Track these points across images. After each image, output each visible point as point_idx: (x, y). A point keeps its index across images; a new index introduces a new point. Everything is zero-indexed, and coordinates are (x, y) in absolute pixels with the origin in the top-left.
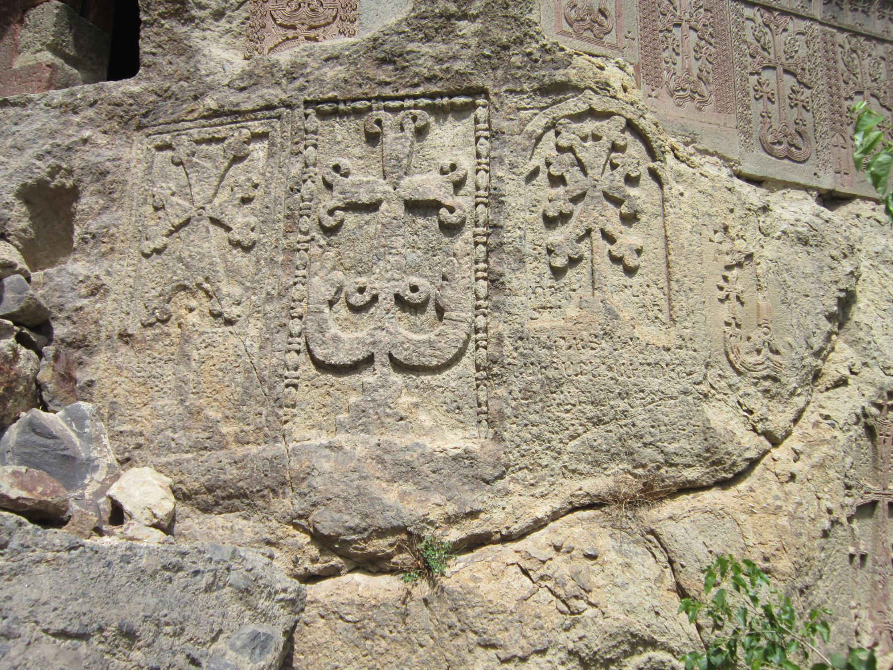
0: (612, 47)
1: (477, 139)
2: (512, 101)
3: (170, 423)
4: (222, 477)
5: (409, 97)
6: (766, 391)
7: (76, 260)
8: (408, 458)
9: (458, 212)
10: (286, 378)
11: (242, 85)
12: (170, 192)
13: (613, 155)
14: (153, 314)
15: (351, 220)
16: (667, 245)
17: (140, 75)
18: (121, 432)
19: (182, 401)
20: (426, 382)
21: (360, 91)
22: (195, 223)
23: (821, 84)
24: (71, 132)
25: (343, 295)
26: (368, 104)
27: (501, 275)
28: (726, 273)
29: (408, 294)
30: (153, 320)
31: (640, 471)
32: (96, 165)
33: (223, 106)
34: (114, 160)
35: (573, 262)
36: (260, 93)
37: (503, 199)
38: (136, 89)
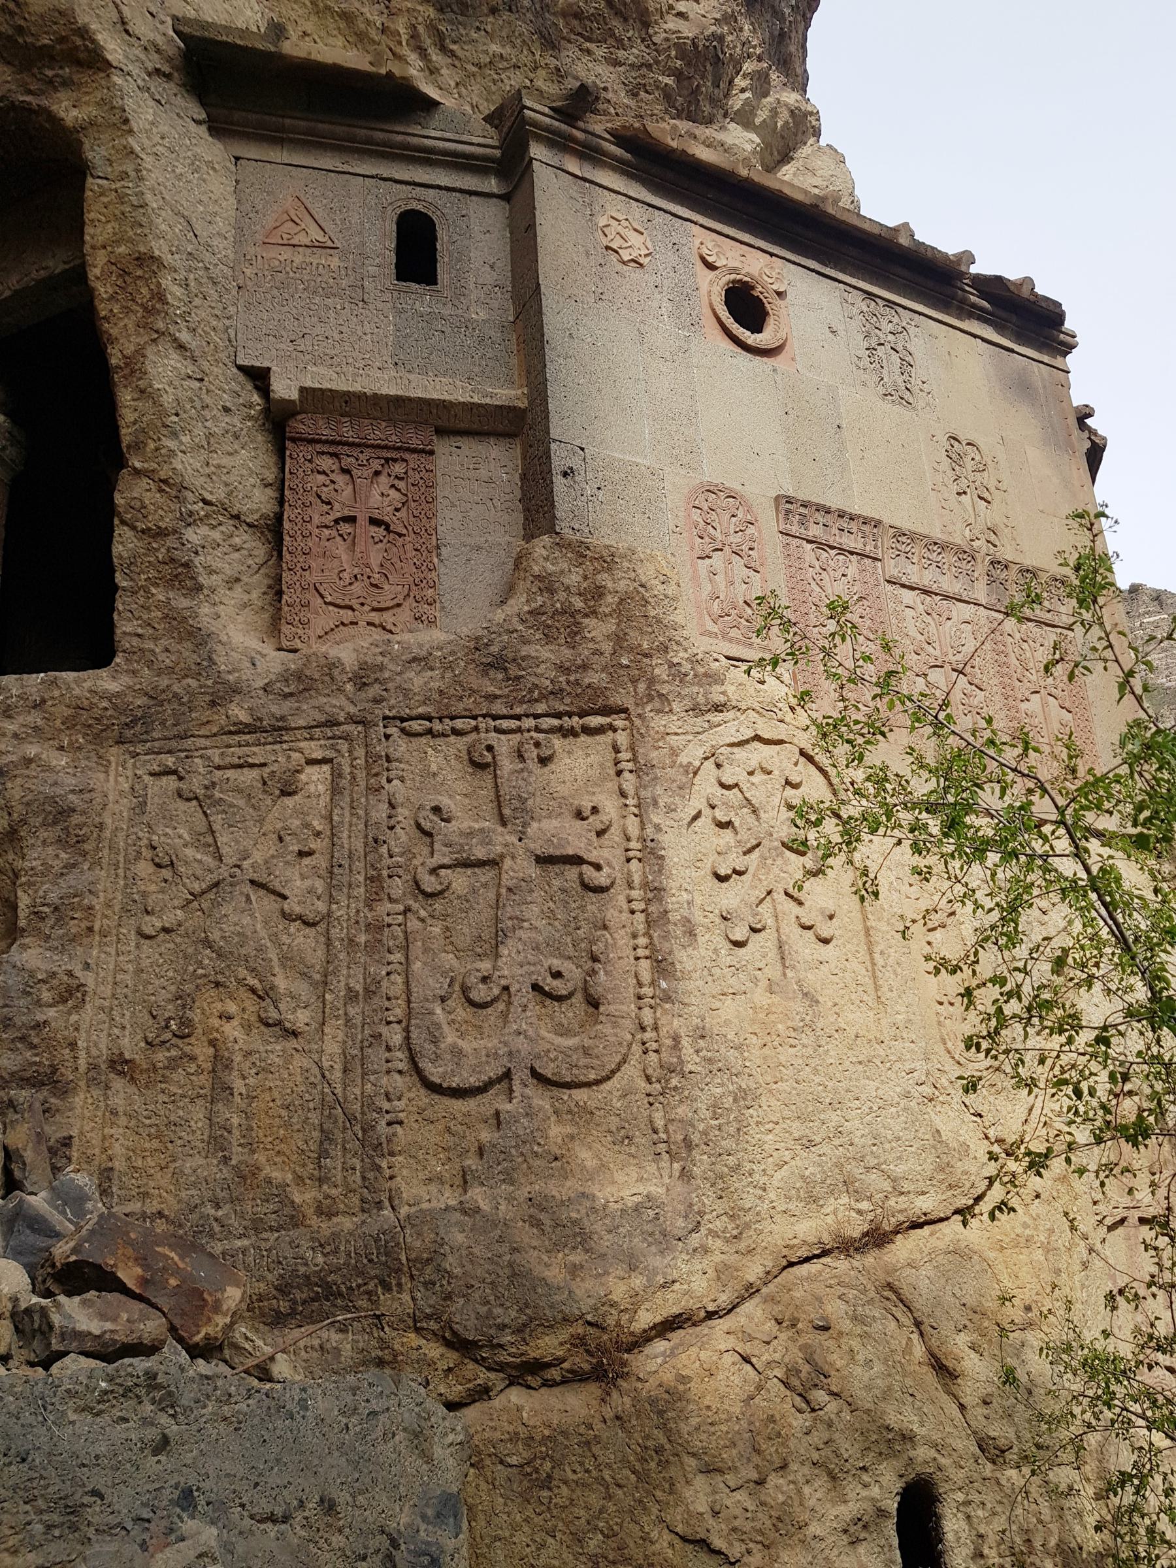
3: (208, 1194)
7: (25, 947)
8: (574, 1215)
10: (387, 1112)
11: (287, 690)
14: (167, 1027)
15: (460, 881)
17: (117, 665)
19: (226, 1160)
21: (461, 706)
22: (228, 889)
25: (457, 988)
26: (473, 723)
29: (550, 984)
30: (167, 1036)
32: (52, 800)
33: (261, 720)
38: (113, 686)
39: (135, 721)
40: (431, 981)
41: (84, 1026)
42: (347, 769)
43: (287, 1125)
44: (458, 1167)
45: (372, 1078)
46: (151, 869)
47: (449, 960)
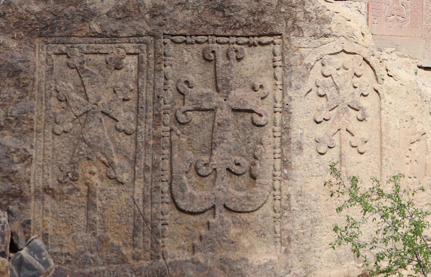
1: (275, 67)
3: (88, 248)
8: (239, 267)
9: (264, 117)
11: (118, 16)
14: (67, 176)
18: (55, 253)
19: (94, 234)
20: (245, 220)
21: (201, 29)
25: (193, 167)
26: (206, 38)
27: (290, 158)
30: (67, 179)
32: (10, 65)
33: (106, 32)
34: (24, 61)
37: (291, 111)
39: (47, 26)
40: (181, 164)
41: (32, 173)
42: (145, 59)
43: (120, 222)
44: (191, 243)
45: (156, 205)
46: (57, 102)
47: (190, 154)
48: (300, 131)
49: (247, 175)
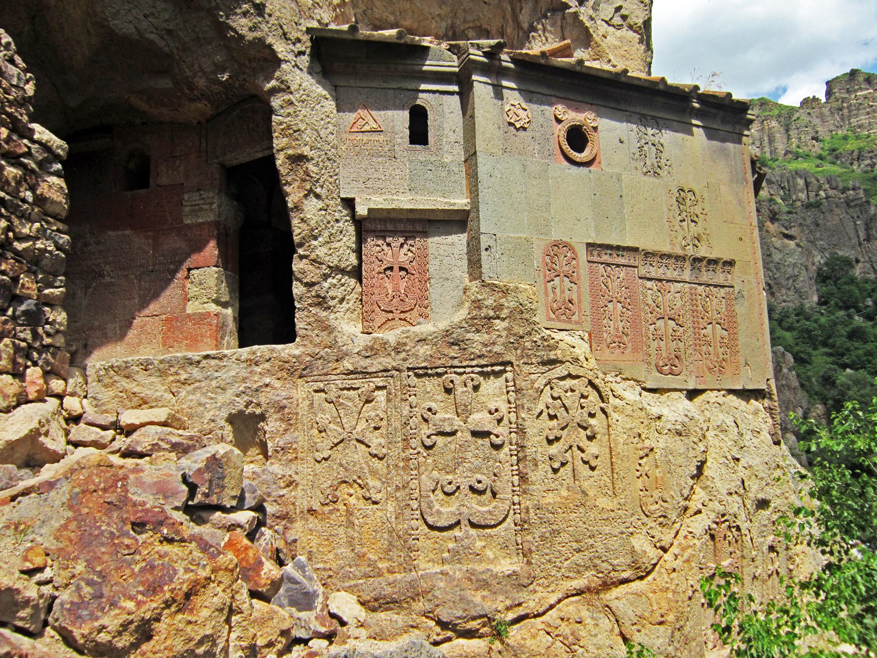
0: (576, 323)
1: (508, 392)
2: (526, 369)
4: (383, 593)
5: (468, 366)
6: (661, 523)
7: (272, 464)
9: (501, 437)
12: (327, 421)
13: (582, 400)
15: (440, 440)
16: (611, 452)
19: (353, 550)
21: (440, 362)
23: (689, 324)
24: (256, 379)
28: (640, 461)
30: (328, 501)
31: (600, 575)
35: (563, 464)
36: (378, 360)
38: (297, 352)
48: (535, 449)
49: (488, 492)
